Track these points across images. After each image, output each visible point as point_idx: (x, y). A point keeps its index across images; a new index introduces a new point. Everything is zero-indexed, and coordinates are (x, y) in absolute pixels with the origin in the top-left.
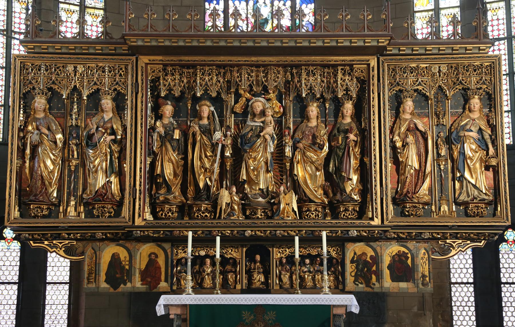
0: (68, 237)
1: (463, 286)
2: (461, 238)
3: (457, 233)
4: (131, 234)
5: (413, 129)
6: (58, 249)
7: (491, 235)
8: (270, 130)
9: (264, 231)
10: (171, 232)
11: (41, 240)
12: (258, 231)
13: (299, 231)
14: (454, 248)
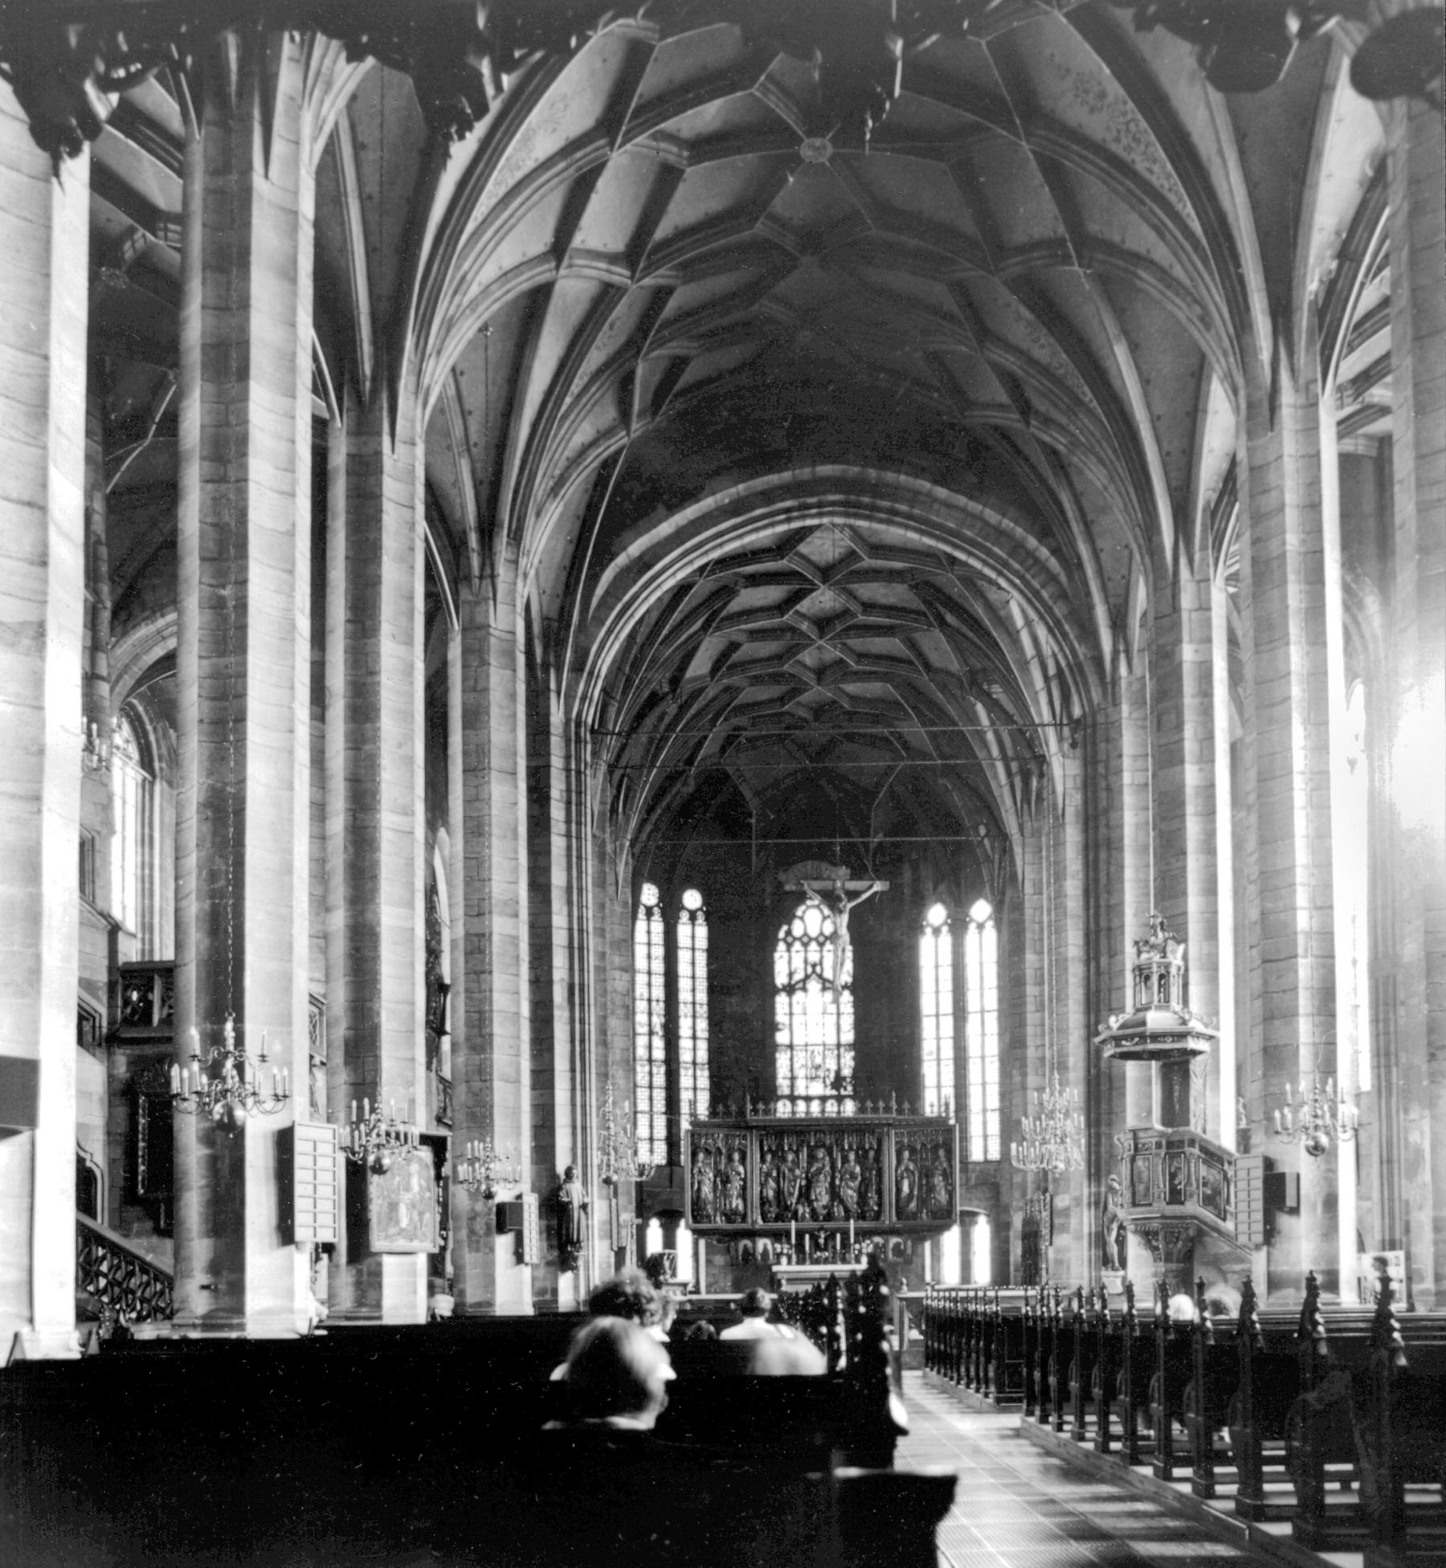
5: (907, 1169)
8: (828, 1168)
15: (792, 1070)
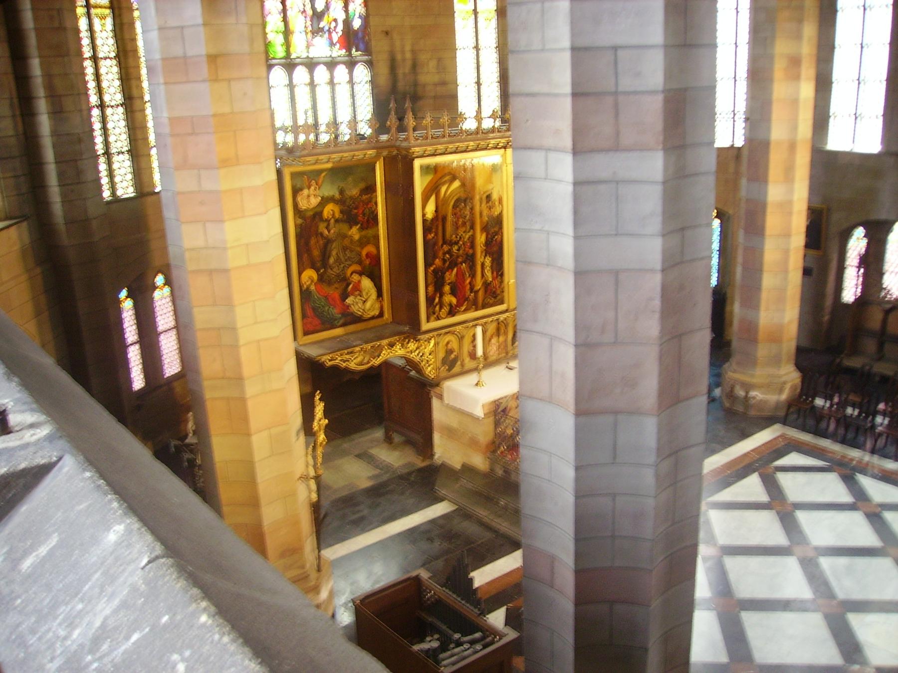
15: (285, 20)
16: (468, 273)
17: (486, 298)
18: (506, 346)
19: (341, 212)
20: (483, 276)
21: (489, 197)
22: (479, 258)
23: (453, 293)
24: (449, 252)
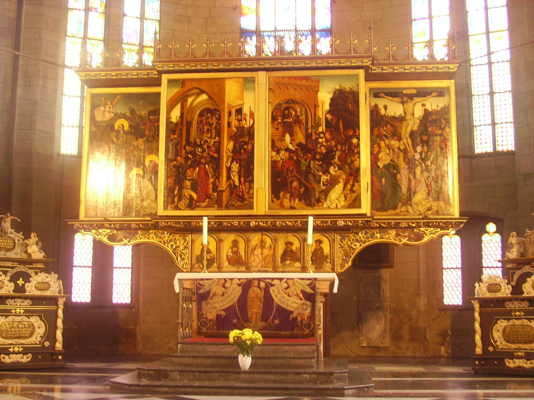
0: (110, 227)
1: (452, 270)
2: (433, 226)
3: (429, 223)
4: (157, 224)
6: (103, 236)
7: (457, 224)
9: (266, 222)
10: (189, 223)
11: (89, 229)
12: (261, 222)
13: (295, 222)
14: (426, 235)
16: (211, 174)
17: (230, 200)
18: (274, 261)
19: (130, 126)
20: (229, 177)
21: (239, 111)
22: (225, 162)
23: (194, 188)
24: (193, 153)
